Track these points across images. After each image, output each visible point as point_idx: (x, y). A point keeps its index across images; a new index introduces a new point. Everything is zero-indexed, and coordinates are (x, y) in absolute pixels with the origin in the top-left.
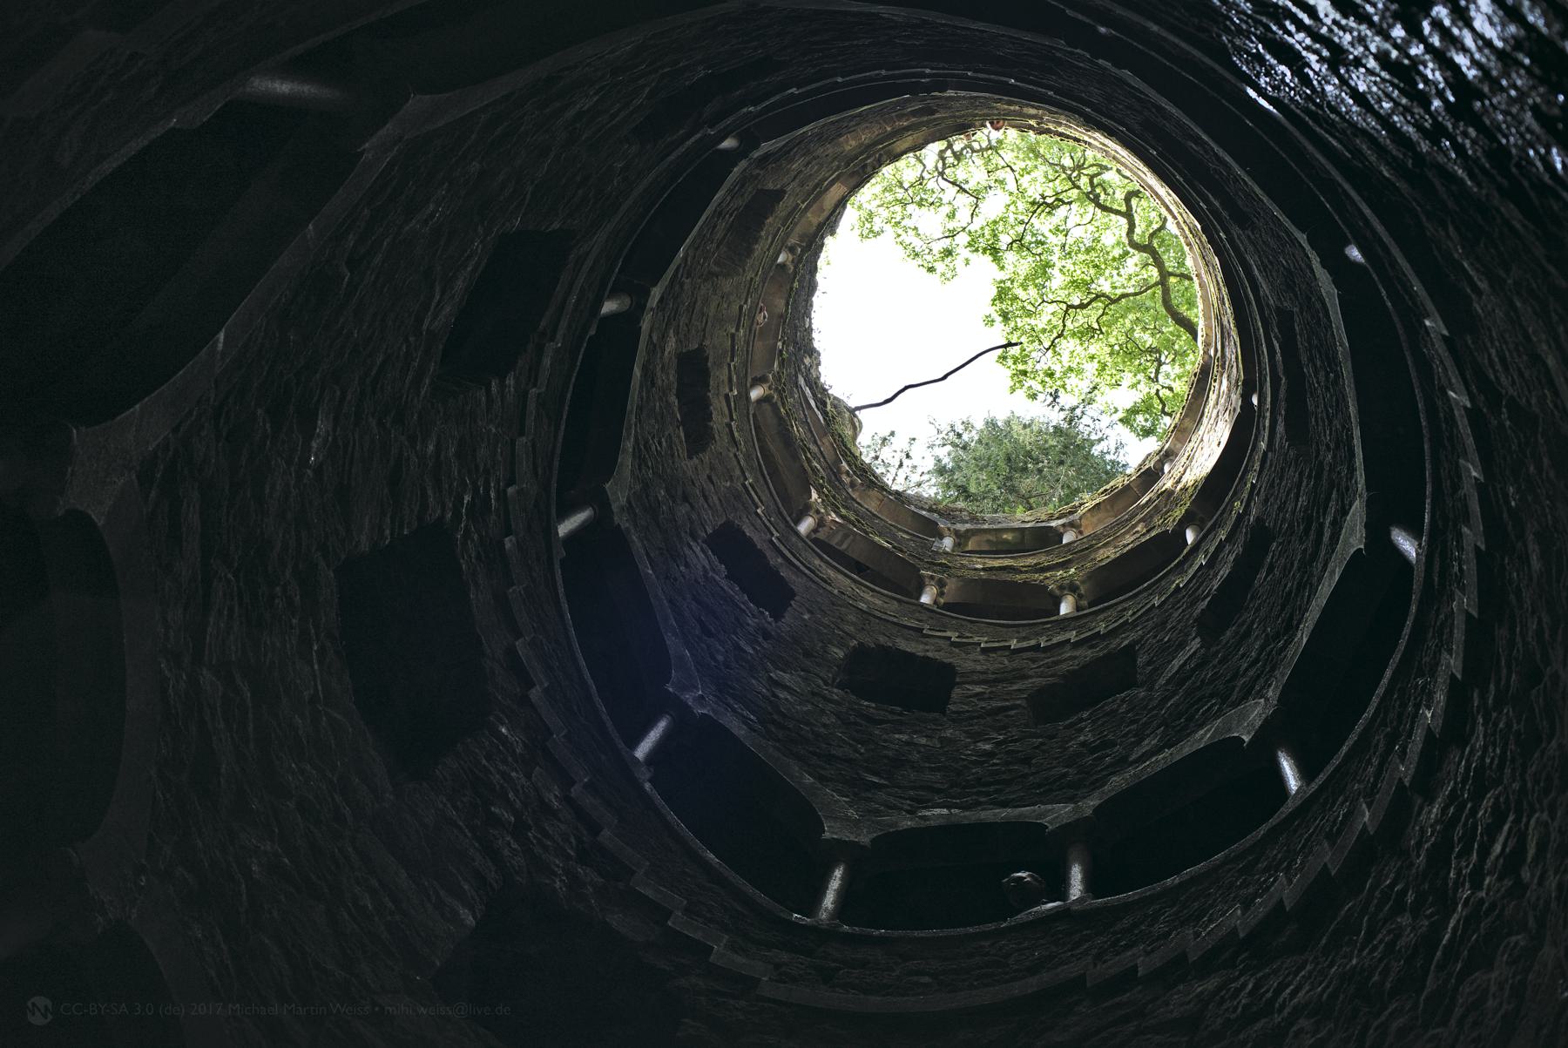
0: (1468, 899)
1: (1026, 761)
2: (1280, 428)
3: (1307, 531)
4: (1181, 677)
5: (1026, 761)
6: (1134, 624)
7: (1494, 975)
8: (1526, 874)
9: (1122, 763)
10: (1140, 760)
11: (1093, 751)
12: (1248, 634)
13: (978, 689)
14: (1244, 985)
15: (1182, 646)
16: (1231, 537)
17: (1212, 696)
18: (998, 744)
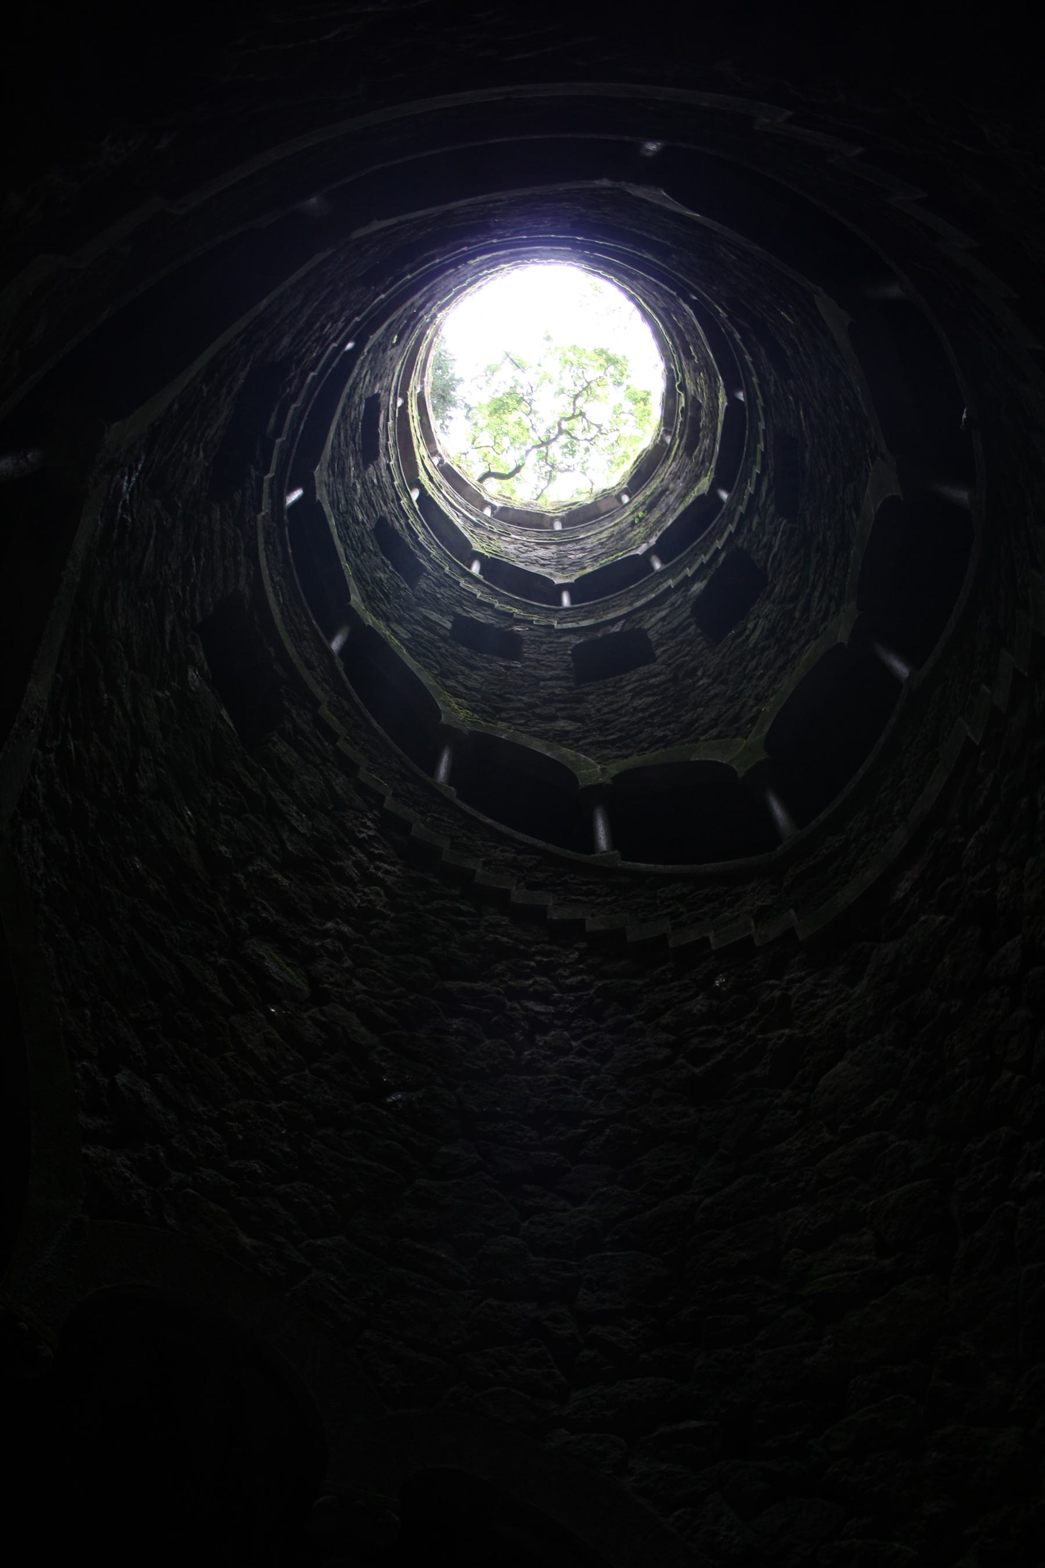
0: (499, 993)
1: (363, 550)
2: (576, 640)
4: (430, 625)
5: (363, 550)
6: (431, 561)
7: (487, 1042)
9: (387, 619)
10: (395, 633)
11: (382, 591)
12: (472, 668)
13: (375, 481)
14: (369, 828)
15: (442, 613)
17: (438, 662)
18: (363, 522)
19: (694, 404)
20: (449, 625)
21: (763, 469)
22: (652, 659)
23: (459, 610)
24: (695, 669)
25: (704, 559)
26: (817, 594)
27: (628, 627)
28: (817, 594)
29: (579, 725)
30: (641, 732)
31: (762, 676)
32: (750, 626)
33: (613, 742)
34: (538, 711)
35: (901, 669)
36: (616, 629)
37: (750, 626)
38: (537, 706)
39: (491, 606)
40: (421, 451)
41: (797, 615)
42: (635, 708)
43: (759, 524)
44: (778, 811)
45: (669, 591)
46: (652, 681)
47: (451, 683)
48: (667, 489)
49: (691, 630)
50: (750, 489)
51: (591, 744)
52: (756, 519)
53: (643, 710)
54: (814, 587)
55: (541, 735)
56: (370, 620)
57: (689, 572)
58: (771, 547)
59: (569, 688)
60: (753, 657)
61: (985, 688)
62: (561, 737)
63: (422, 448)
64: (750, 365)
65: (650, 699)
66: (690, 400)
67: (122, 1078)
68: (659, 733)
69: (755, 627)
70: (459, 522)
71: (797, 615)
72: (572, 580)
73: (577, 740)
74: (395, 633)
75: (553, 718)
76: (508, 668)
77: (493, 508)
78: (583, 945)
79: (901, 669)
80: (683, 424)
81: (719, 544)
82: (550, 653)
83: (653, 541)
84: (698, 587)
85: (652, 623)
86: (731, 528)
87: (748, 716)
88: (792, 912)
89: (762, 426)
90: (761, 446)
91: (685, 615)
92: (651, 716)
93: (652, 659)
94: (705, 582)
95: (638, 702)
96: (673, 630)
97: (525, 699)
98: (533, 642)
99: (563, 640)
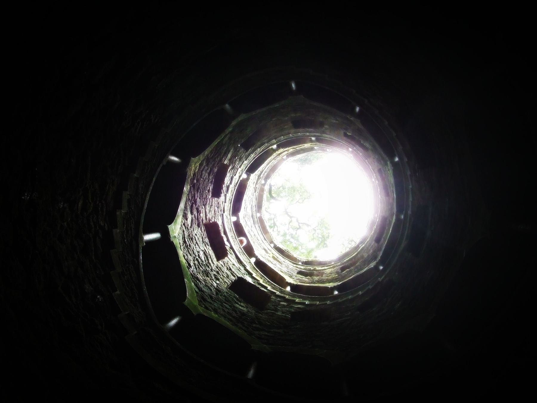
2: (220, 223)
3: (197, 209)
15: (230, 160)
16: (228, 187)
19: (320, 273)
20: (226, 162)
22: (218, 260)
23: (230, 168)
24: (218, 280)
26: (266, 333)
28: (266, 333)
29: (190, 225)
30: (190, 255)
31: (224, 311)
32: (242, 304)
33: (185, 242)
34: (194, 205)
35: (251, 374)
37: (242, 304)
38: (196, 205)
39: (231, 183)
40: (291, 149)
41: (254, 325)
42: (198, 252)
43: (284, 305)
44: (174, 322)
46: (210, 259)
47: (204, 164)
48: (281, 264)
49: (232, 277)
50: (297, 300)
51: (184, 231)
52: (285, 304)
53: (199, 255)
55: (186, 208)
56: (234, 123)
57: (254, 275)
59: (202, 220)
60: (230, 306)
63: (292, 150)
64: (357, 294)
65: (203, 259)
68: (192, 264)
69: (242, 307)
70: (260, 169)
71: (254, 325)
72: (242, 222)
73: (184, 224)
74: (225, 136)
75: (192, 213)
76: (209, 191)
77: (264, 185)
79: (251, 374)
80: (310, 270)
81: (269, 288)
82: (215, 211)
83: (262, 259)
84: (250, 280)
85: (230, 259)
86: (278, 293)
87: (207, 306)
88: (136, 332)
89: (328, 302)
91: (238, 274)
92: (197, 260)
93: (218, 260)
95: (201, 254)
96: (230, 269)
97: (198, 200)
98: (218, 203)
99: (220, 217)
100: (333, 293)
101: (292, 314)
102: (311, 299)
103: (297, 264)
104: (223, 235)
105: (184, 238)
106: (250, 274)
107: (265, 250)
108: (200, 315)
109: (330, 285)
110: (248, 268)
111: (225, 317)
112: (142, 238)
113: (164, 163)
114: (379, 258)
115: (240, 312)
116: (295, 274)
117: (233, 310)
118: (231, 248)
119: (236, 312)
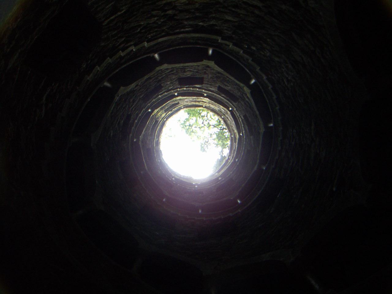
2: (234, 103)
8: (289, 78)
21: (159, 95)
25: (191, 89)
27: (221, 93)
28: (166, 73)
36: (223, 95)
41: (175, 71)
45: (205, 90)
52: (170, 88)
54: (165, 74)
57: (197, 89)
58: (170, 83)
61: (134, 50)
62: (247, 97)
66: (167, 112)
67: (334, 189)
68: (227, 78)
69: (188, 74)
78: (270, 76)
81: (185, 89)
86: (178, 89)
90: (154, 100)
94: (195, 86)
95: (228, 85)
96: (210, 85)
100: (151, 109)
101: (162, 87)
102: (159, 99)
103: (184, 105)
104: (228, 98)
105: (242, 89)
106: (199, 88)
107: (205, 102)
108: (202, 61)
109: (156, 111)
110: (204, 91)
111: (191, 66)
112: (255, 79)
113: (272, 120)
114: (140, 143)
115: (187, 72)
116: (180, 102)
117: (191, 70)
118: (219, 95)
119: (189, 71)
